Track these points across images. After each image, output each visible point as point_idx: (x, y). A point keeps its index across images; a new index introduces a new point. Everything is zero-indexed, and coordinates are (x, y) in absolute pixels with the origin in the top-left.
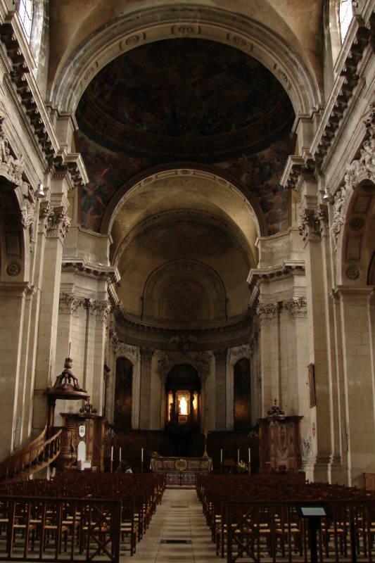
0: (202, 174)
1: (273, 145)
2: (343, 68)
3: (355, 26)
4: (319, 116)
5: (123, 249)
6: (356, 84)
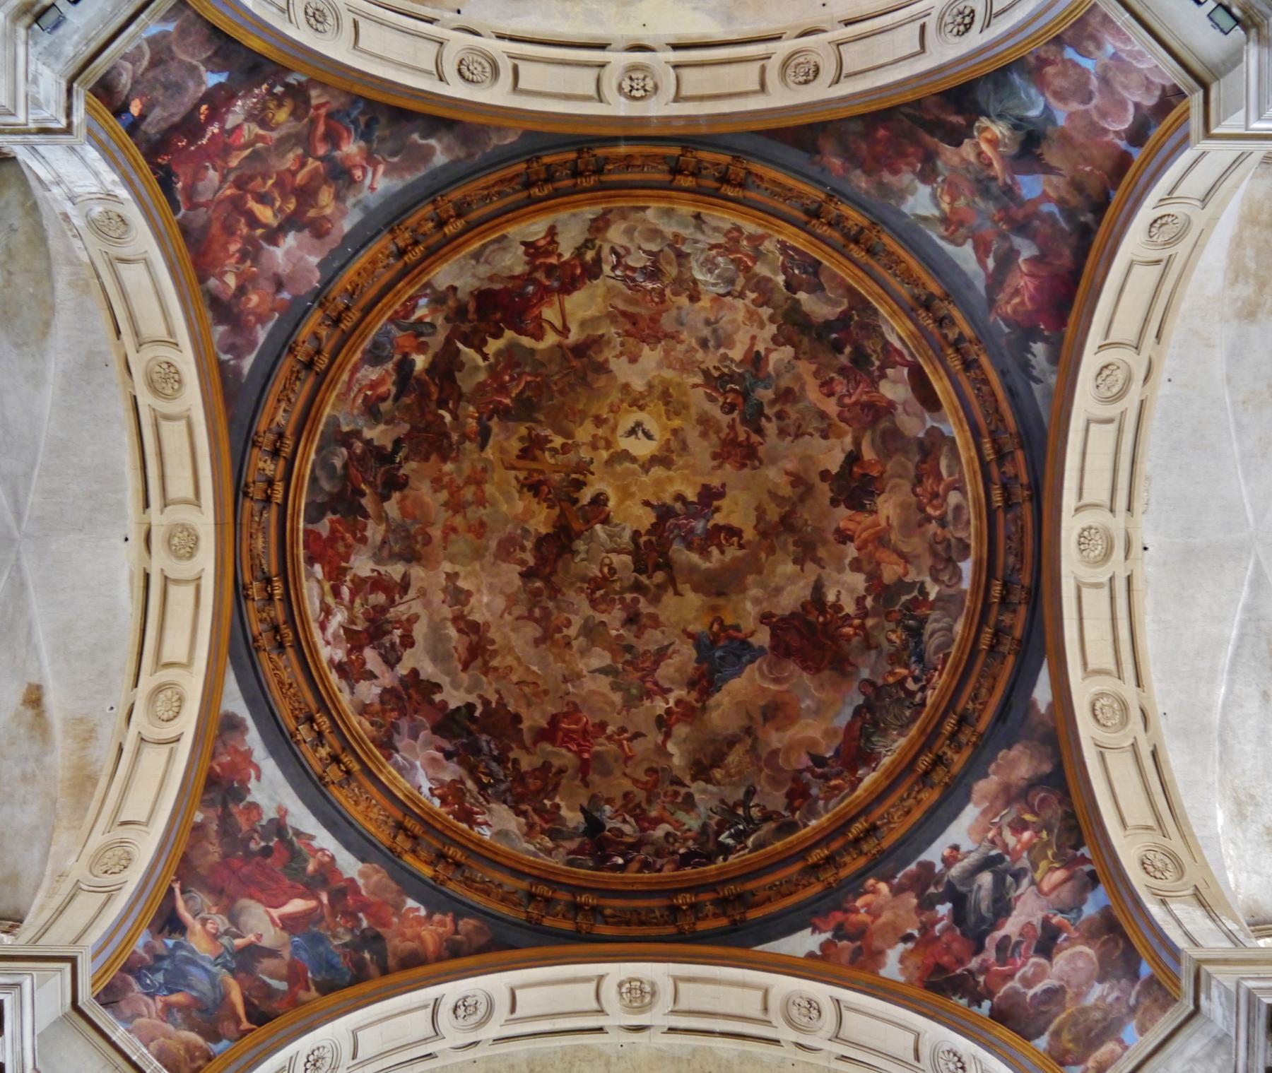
1: (985, 786)
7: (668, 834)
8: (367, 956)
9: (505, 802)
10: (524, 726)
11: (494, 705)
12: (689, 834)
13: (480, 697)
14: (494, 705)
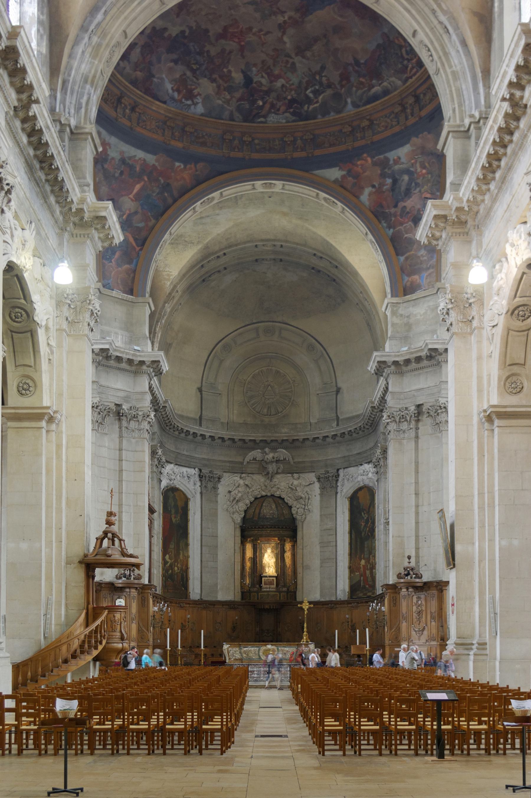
0: (296, 189)
2: (504, 92)
3: (519, 39)
4: (479, 129)
5: (169, 310)
6: (524, 113)
7: (283, 86)
8: (166, 194)
9: (205, 77)
10: (210, 34)
11: (194, 28)
12: (293, 87)
13: (187, 26)
14: (194, 28)
